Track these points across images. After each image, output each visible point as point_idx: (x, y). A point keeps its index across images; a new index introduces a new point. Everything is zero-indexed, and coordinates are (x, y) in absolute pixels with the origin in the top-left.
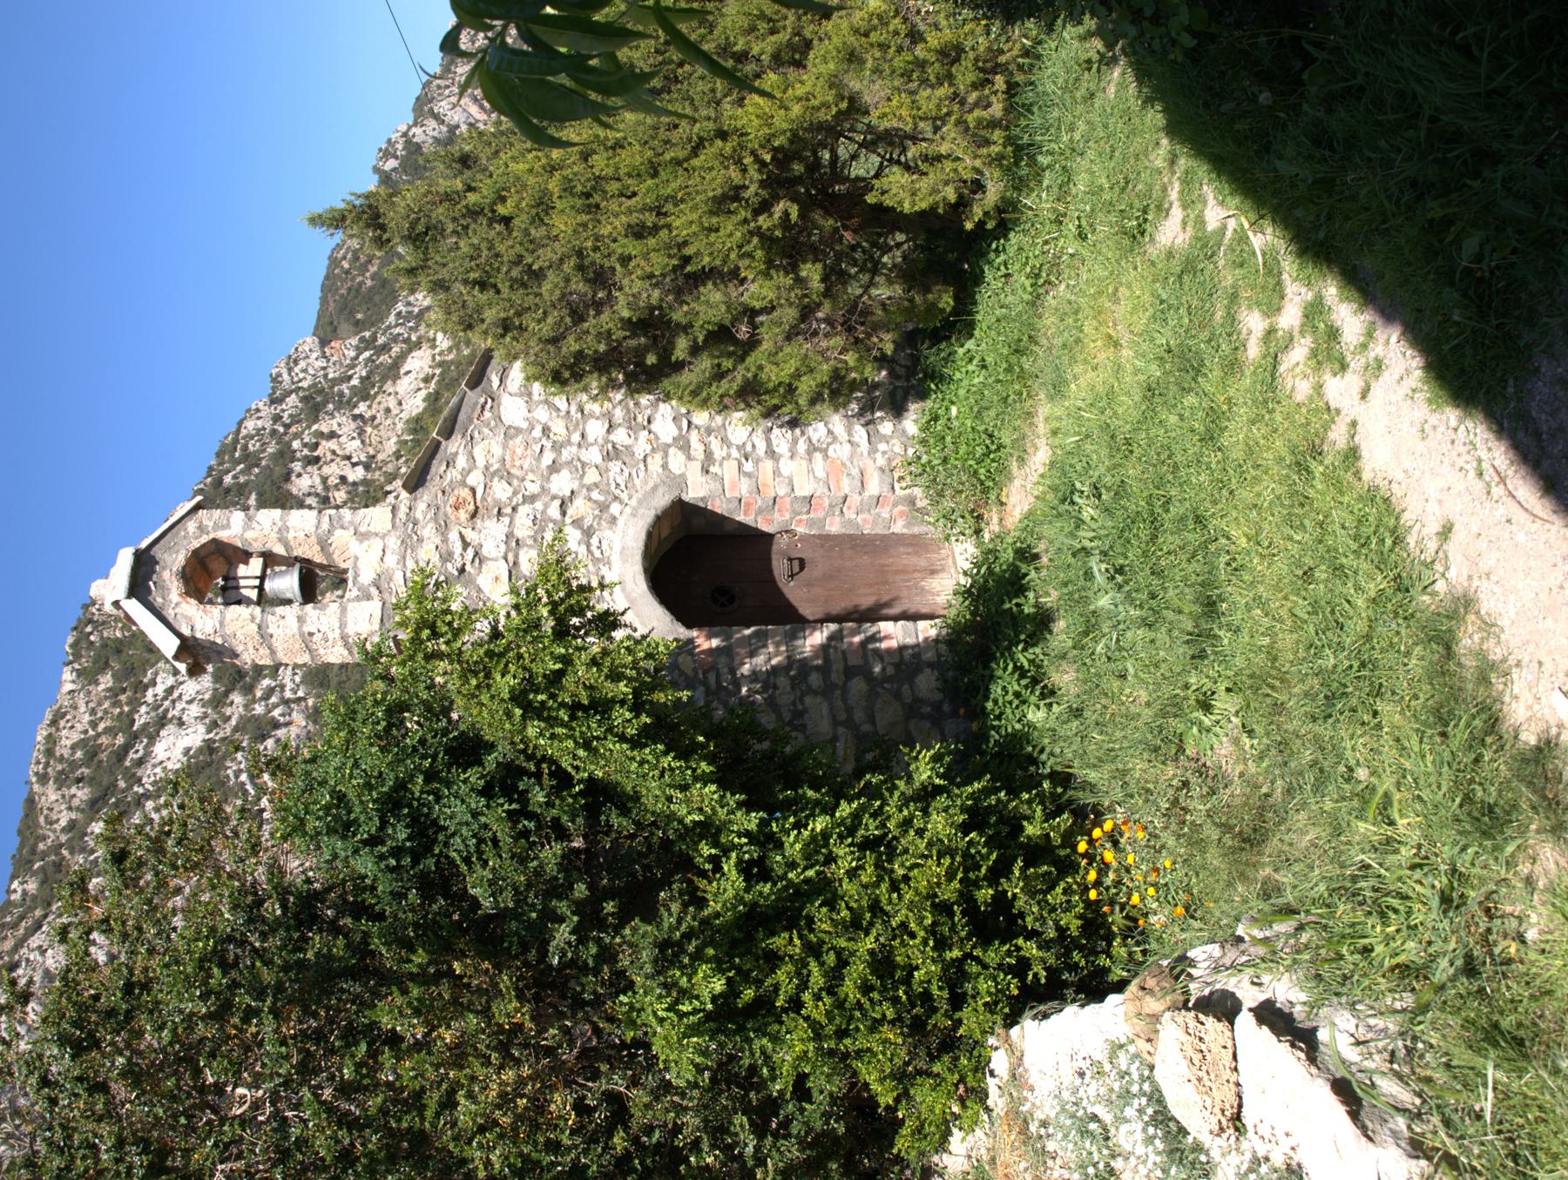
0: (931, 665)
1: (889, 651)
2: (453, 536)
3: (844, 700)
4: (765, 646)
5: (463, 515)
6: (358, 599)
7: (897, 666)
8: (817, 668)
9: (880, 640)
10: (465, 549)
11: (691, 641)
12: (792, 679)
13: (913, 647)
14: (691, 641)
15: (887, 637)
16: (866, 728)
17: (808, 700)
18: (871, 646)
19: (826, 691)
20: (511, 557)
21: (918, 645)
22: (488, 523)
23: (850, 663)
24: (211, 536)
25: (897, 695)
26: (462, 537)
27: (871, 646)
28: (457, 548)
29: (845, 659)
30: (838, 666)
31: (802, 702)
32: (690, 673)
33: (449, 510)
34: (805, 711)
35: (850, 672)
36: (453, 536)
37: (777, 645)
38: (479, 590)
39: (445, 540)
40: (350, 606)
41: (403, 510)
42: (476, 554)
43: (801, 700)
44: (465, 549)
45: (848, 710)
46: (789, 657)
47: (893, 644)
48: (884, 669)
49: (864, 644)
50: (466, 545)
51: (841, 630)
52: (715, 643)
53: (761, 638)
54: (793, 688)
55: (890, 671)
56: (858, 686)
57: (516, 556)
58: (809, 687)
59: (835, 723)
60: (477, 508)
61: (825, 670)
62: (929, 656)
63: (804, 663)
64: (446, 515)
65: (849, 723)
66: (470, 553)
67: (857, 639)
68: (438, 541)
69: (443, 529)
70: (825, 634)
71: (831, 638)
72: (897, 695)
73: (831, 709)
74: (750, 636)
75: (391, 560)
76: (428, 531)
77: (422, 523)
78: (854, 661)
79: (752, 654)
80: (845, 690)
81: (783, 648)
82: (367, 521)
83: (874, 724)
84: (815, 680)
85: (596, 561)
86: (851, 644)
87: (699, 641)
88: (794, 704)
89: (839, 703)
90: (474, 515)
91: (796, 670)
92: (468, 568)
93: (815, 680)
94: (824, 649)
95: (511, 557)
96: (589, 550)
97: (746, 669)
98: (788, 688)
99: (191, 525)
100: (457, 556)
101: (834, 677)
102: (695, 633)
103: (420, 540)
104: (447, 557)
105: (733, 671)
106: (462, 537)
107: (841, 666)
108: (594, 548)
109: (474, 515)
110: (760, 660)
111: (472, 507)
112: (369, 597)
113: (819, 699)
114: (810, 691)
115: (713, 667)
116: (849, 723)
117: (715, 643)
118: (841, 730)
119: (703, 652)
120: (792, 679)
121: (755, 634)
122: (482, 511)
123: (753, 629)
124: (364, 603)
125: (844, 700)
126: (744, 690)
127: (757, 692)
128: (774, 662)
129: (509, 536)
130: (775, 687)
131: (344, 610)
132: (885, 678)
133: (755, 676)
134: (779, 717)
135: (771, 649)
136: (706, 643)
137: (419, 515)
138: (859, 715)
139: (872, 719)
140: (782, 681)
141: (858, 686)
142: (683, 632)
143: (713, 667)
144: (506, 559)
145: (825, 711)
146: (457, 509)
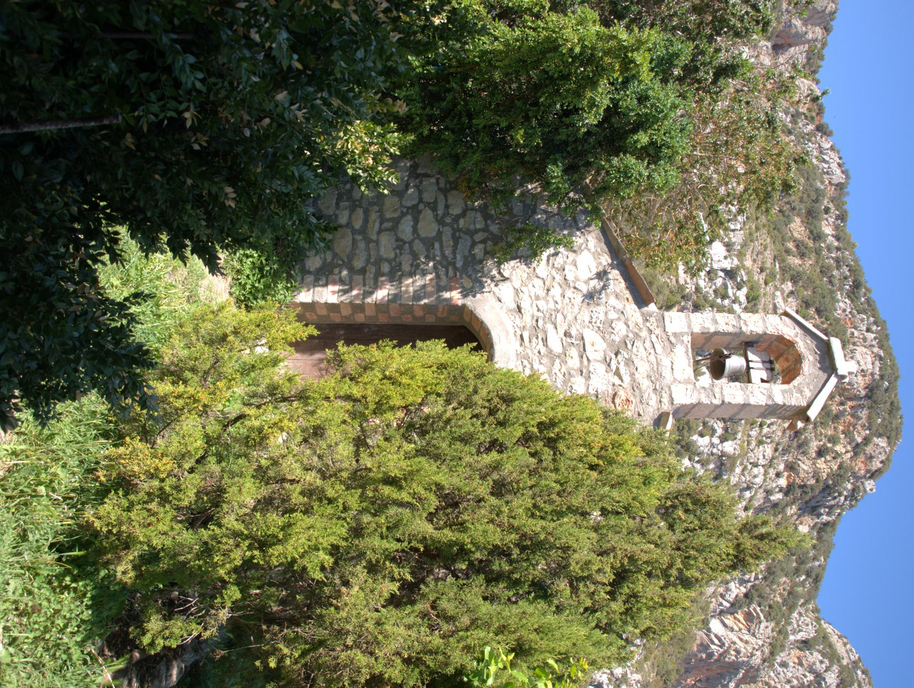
0: (309, 272)
1: (334, 283)
2: (627, 379)
3: (369, 256)
4: (415, 291)
5: (622, 394)
6: (682, 334)
7: (331, 273)
8: (383, 275)
9: (339, 291)
10: (617, 369)
11: (465, 296)
12: (400, 270)
13: (319, 286)
14: (465, 296)
15: (334, 292)
16: (359, 237)
17: (392, 255)
18: (347, 287)
19: (379, 261)
20: (585, 360)
21: (314, 286)
22: (604, 388)
23: (361, 277)
24: (791, 385)
25: (335, 255)
26: (621, 378)
27: (347, 287)
28: (623, 370)
29: (364, 280)
30: (370, 275)
31: (396, 254)
32: (464, 276)
33: (632, 399)
34: (394, 249)
35: (363, 271)
36: (627, 379)
37: (407, 292)
38: (604, 338)
39: (632, 375)
40: (686, 330)
41: (666, 400)
42: (609, 365)
43: (396, 256)
44: (617, 369)
45: (368, 249)
46: (401, 283)
47: (331, 288)
48: (340, 273)
49: (351, 290)
50: (617, 373)
51: (364, 298)
52: (447, 295)
53: (417, 297)
54: (400, 263)
55: (336, 271)
56: (358, 264)
57: (581, 362)
58: (390, 264)
59: (377, 242)
60: (613, 402)
61: (379, 274)
62: (310, 279)
63: (391, 280)
64: (634, 396)
65: (368, 241)
66: (614, 367)
67: (355, 292)
68: (637, 376)
69: (635, 386)
70: (374, 296)
71: (371, 293)
72: (335, 255)
73: (378, 250)
74: (425, 298)
75: (666, 362)
76: (645, 384)
77: (650, 390)
78: (359, 278)
79: (424, 286)
80: (368, 261)
81: (403, 289)
82: (689, 393)
83: (354, 239)
84: (386, 268)
85: (527, 357)
86: (360, 290)
87: (459, 296)
88: (401, 254)
89: (372, 253)
90: (615, 395)
91: (396, 275)
92: (613, 356)
93: (386, 268)
94: (376, 286)
95: (585, 360)
96: (532, 365)
97: (429, 277)
98: (403, 263)
99: (808, 394)
100: (622, 363)
101: (373, 270)
102: (460, 303)
103: (649, 377)
104: (629, 362)
105: (438, 276)
106: (621, 378)
107: (367, 274)
108: (529, 366)
109: (615, 395)
110: (420, 283)
111: (617, 401)
112: (675, 335)
113: (385, 256)
114: (389, 261)
115: (450, 279)
116: (368, 241)
117: (447, 295)
118: (374, 237)
119: (456, 289)
120: (400, 270)
121: (420, 299)
122: (609, 399)
123: (422, 302)
124: (678, 331)
125: (369, 256)
126: (431, 264)
127: (424, 263)
128: (410, 281)
129: (588, 378)
130: (412, 265)
131: (689, 326)
132: (341, 267)
133: (424, 274)
134: (411, 248)
135: (411, 289)
136: (455, 296)
137: (653, 396)
138: (362, 245)
139: (354, 242)
140: (406, 267)
141: (358, 264)
142: (469, 302)
143: (450, 279)
144: (588, 359)
145: (382, 249)
146: (628, 400)
